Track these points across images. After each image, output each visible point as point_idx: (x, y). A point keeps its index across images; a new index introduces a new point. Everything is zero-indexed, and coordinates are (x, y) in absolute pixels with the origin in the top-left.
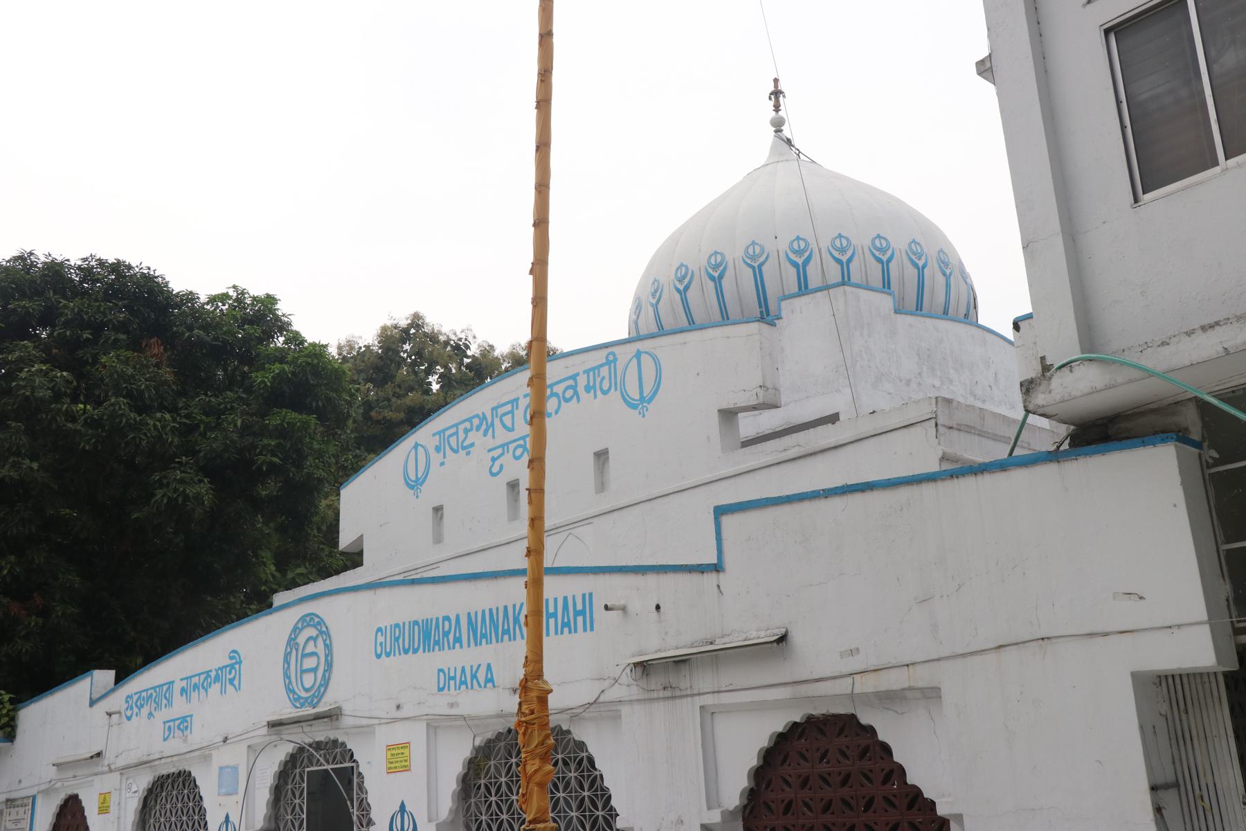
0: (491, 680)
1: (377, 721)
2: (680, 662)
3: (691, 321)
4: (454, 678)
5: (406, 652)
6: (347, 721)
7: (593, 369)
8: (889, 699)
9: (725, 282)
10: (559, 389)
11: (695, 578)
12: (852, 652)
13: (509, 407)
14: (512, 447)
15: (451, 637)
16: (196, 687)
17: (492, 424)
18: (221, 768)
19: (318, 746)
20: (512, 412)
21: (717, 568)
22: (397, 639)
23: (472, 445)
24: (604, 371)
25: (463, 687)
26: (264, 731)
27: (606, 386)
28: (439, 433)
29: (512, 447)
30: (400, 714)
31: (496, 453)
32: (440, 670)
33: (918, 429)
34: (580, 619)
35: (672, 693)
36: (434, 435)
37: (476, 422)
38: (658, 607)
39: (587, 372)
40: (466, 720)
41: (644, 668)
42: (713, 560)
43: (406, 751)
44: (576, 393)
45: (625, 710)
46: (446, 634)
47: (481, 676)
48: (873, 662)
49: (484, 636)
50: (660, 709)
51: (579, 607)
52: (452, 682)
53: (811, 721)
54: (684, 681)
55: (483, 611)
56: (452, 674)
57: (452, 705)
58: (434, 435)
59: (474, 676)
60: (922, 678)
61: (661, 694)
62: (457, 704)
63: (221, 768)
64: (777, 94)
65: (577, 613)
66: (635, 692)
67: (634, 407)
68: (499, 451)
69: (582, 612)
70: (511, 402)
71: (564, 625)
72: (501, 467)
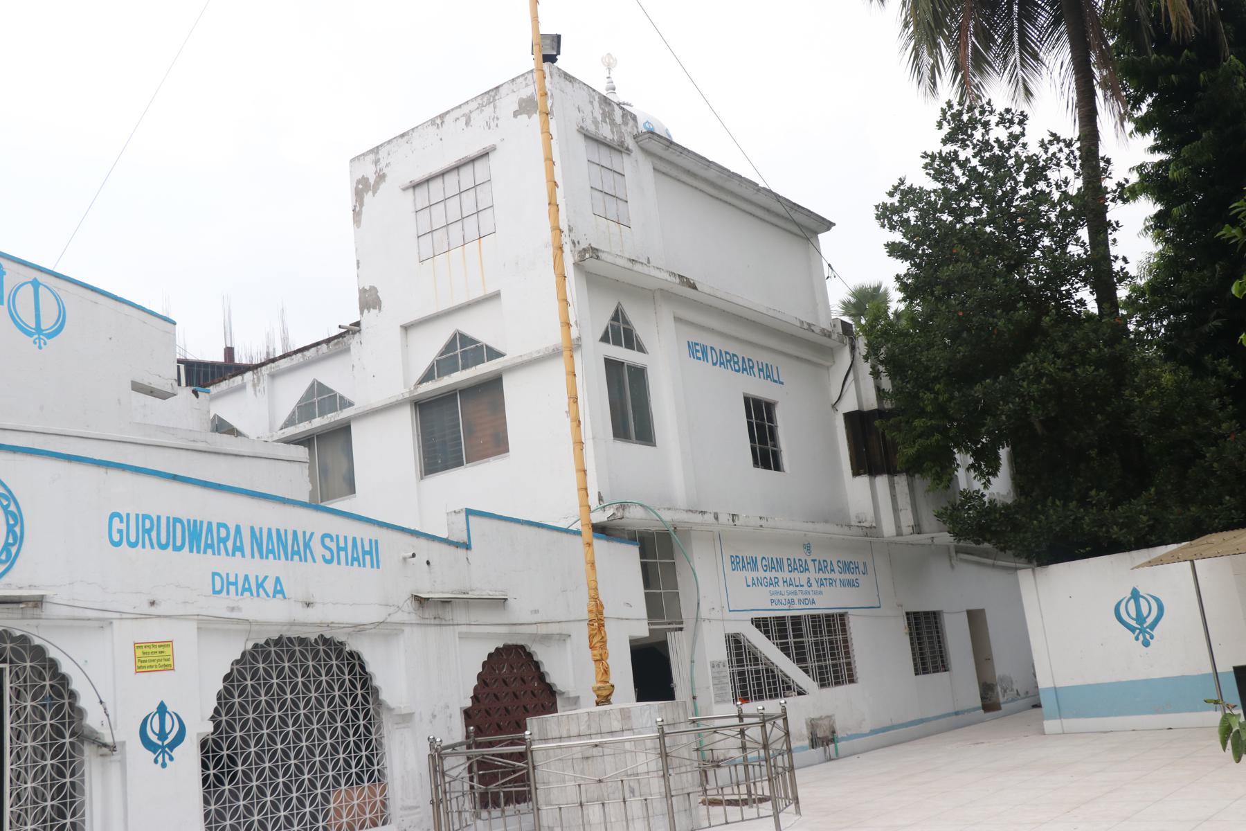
0: (282, 592)
1: (117, 615)
2: (445, 602)
4: (235, 584)
6: (49, 610)
8: (546, 638)
11: (452, 549)
12: (536, 612)
15: (230, 544)
21: (467, 546)
22: (149, 531)
25: (247, 594)
30: (153, 611)
32: (214, 574)
33: (296, 465)
34: (368, 558)
35: (440, 622)
38: (428, 563)
41: (421, 601)
42: (466, 539)
43: (168, 651)
45: (407, 629)
47: (269, 586)
48: (545, 619)
49: (269, 551)
50: (432, 632)
51: (367, 548)
52: (232, 588)
54: (448, 614)
55: (269, 530)
56: (232, 579)
57: (233, 609)
59: (260, 586)
60: (564, 628)
61: (433, 622)
62: (239, 609)
65: (365, 553)
66: (413, 618)
67: (30, 334)
69: (370, 553)
71: (354, 559)
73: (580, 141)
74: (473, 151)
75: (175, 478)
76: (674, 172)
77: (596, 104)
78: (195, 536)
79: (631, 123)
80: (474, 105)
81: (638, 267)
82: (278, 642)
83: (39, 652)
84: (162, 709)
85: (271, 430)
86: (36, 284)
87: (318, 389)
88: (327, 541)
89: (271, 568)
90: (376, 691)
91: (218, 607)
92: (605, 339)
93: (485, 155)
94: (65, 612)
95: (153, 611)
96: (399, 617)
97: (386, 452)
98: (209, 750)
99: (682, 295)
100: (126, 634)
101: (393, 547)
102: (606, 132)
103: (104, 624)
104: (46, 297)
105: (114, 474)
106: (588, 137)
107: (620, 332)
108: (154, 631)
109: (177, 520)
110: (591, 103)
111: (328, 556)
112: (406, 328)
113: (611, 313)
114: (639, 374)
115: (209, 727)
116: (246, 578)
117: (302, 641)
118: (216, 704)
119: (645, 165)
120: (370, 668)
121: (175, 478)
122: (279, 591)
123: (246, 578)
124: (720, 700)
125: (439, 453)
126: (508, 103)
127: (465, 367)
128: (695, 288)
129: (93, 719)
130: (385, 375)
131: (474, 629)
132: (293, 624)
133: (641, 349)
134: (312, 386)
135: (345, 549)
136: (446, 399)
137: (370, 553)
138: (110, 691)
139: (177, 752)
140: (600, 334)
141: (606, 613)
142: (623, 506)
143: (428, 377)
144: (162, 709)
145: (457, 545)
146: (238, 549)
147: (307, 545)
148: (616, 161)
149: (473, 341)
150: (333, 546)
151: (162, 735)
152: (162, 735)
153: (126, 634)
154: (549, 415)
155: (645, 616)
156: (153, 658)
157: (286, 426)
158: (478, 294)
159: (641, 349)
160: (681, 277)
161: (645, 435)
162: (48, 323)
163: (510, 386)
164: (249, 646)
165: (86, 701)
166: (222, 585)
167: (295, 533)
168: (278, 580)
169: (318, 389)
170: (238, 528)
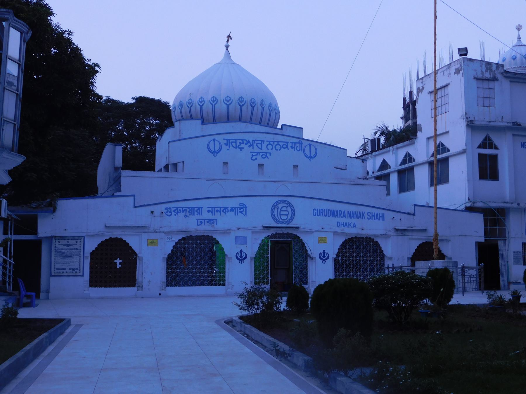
2: (405, 230)
3: (268, 124)
5: (325, 216)
6: (300, 229)
7: (294, 143)
9: (255, 109)
10: (281, 144)
11: (408, 216)
13: (260, 142)
14: (261, 154)
15: (342, 215)
16: (217, 211)
17: (253, 145)
18: (236, 237)
19: (280, 234)
20: (261, 144)
23: (243, 148)
24: (298, 145)
26: (262, 228)
27: (298, 149)
29: (261, 154)
30: (323, 230)
31: (254, 154)
36: (224, 139)
37: (245, 142)
39: (292, 143)
40: (346, 234)
44: (287, 146)
46: (341, 214)
47: (352, 225)
53: (426, 242)
58: (224, 139)
63: (236, 237)
64: (229, 37)
65: (380, 217)
68: (256, 154)
69: (382, 217)
70: (262, 141)
72: (256, 159)
73: (475, 82)
74: (444, 84)
75: (329, 200)
76: (521, 81)
77: (484, 66)
78: (333, 213)
79: (501, 68)
80: (445, 68)
81: (492, 124)
82: (356, 237)
83: (299, 237)
84: (324, 251)
85: (396, 166)
86: (310, 145)
87: (408, 154)
88: (369, 214)
89: (353, 221)
91: (338, 230)
93: (447, 85)
94: (303, 230)
95: (323, 230)
96: (390, 233)
98: (336, 260)
99: (515, 127)
100: (316, 235)
101: (389, 215)
102: (487, 75)
103: (312, 232)
104: (312, 147)
105: (316, 200)
106: (477, 79)
107: (487, 143)
108: (323, 235)
109: (329, 210)
110: (481, 66)
111: (369, 217)
112: (428, 138)
113: (483, 137)
115: (335, 256)
116: (346, 223)
119: (506, 83)
120: (381, 246)
121: (329, 200)
122: (355, 226)
123: (346, 223)
124: (516, 263)
126: (453, 69)
127: (442, 153)
128: (520, 125)
129: (309, 252)
131: (414, 237)
132: (358, 234)
133: (496, 148)
135: (374, 216)
137: (382, 217)
138: (313, 246)
139: (327, 261)
142: (474, 202)
144: (324, 251)
145: (410, 214)
146: (344, 216)
147: (363, 215)
148: (491, 84)
149: (444, 145)
150: (371, 215)
151: (324, 257)
152: (324, 257)
153: (316, 235)
155: (483, 235)
156: (322, 240)
158: (444, 131)
159: (496, 148)
160: (513, 123)
162: (312, 155)
163: (450, 160)
164: (347, 239)
165: (307, 248)
166: (340, 224)
167: (360, 212)
168: (354, 224)
169: (408, 154)
170: (344, 212)
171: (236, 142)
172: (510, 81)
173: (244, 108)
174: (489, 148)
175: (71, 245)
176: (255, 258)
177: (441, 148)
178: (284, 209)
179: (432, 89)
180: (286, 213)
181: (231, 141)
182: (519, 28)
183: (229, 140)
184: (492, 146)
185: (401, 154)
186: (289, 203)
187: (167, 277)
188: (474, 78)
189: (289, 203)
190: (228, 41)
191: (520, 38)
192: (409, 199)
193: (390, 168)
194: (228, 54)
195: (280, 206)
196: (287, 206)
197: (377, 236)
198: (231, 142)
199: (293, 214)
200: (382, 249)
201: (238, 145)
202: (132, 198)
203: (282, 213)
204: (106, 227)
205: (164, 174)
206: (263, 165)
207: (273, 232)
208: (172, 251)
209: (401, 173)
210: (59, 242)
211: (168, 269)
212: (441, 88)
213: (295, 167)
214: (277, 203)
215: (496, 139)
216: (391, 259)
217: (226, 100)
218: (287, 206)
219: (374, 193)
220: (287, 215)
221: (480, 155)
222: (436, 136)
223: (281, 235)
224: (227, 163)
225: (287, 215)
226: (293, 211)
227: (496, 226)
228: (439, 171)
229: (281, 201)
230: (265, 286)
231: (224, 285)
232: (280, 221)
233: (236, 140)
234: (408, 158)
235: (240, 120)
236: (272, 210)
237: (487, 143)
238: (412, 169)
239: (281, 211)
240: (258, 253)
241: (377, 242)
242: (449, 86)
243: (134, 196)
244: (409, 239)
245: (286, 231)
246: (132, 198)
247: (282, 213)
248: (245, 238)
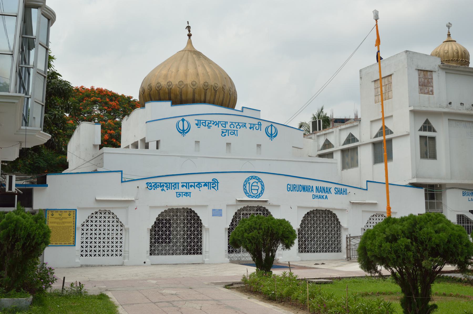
6: (269, 202)
18: (213, 210)
28: (198, 120)
63: (213, 210)
83: (267, 210)
87: (351, 135)
90: (339, 222)
92: (420, 130)
93: (391, 75)
97: (365, 155)
107: (427, 127)
112: (372, 122)
114: (433, 139)
117: (322, 211)
118: (301, 222)
120: (338, 217)
125: (377, 159)
130: (366, 134)
133: (434, 131)
134: (350, 134)
136: (381, 142)
140: (419, 128)
141: (392, 210)
143: (376, 136)
154: (405, 151)
157: (344, 144)
159: (434, 131)
161: (434, 156)
169: (351, 135)
171: (205, 123)
172: (446, 72)
173: (208, 91)
174: (429, 131)
175: (63, 218)
176: (229, 229)
177: (385, 131)
178: (255, 184)
179: (378, 77)
180: (257, 188)
181: (201, 122)
182: (449, 26)
183: (200, 121)
184: (431, 129)
185: (344, 136)
186: (259, 179)
187: (151, 246)
188: (416, 69)
189: (259, 179)
190: (189, 31)
191: (450, 35)
192: (351, 176)
193: (334, 147)
194: (190, 42)
195: (251, 181)
196: (257, 181)
197: (335, 209)
198: (202, 123)
199: (263, 189)
200: (339, 220)
201: (208, 124)
202: (119, 174)
203: (253, 188)
204: (96, 200)
205: (132, 150)
206: (230, 144)
207: (246, 205)
208: (155, 223)
209: (343, 151)
210: (52, 215)
211: (151, 239)
212: (385, 77)
213: (259, 146)
214: (248, 178)
215: (434, 123)
216: (346, 229)
217: (192, 84)
218: (257, 181)
219: (332, 169)
220: (257, 190)
221: (421, 137)
222: (383, 119)
223: (251, 208)
224: (199, 142)
225: (257, 190)
226: (263, 186)
227: (434, 199)
228: (383, 150)
229: (252, 177)
230: (231, 254)
231: (201, 253)
232: (251, 195)
233: (205, 121)
234: (351, 139)
235: (204, 102)
236: (244, 185)
237: (427, 127)
238: (355, 148)
239: (252, 186)
240: (232, 224)
241: (335, 214)
242: (392, 76)
243: (122, 171)
244: (363, 211)
245: (256, 205)
246: (119, 174)
247: (253, 188)
248: (221, 210)
